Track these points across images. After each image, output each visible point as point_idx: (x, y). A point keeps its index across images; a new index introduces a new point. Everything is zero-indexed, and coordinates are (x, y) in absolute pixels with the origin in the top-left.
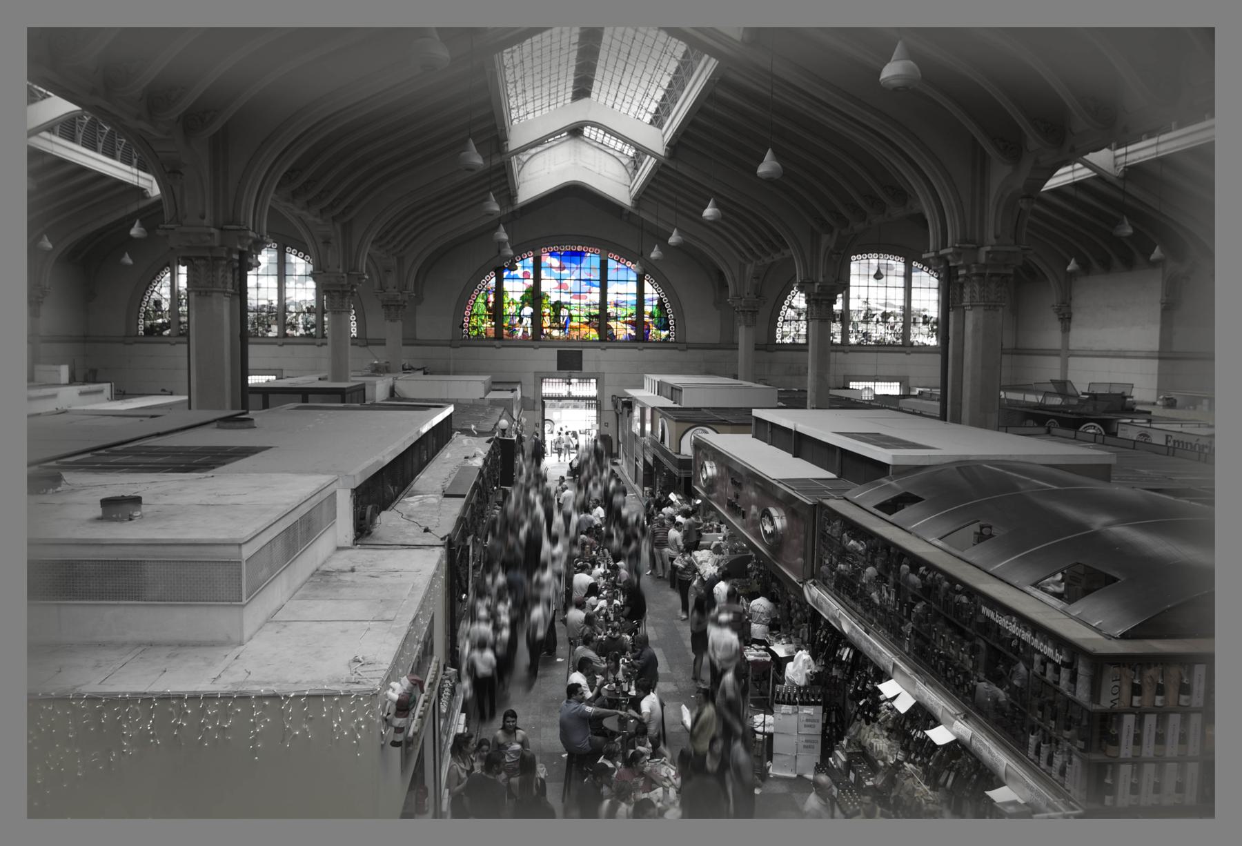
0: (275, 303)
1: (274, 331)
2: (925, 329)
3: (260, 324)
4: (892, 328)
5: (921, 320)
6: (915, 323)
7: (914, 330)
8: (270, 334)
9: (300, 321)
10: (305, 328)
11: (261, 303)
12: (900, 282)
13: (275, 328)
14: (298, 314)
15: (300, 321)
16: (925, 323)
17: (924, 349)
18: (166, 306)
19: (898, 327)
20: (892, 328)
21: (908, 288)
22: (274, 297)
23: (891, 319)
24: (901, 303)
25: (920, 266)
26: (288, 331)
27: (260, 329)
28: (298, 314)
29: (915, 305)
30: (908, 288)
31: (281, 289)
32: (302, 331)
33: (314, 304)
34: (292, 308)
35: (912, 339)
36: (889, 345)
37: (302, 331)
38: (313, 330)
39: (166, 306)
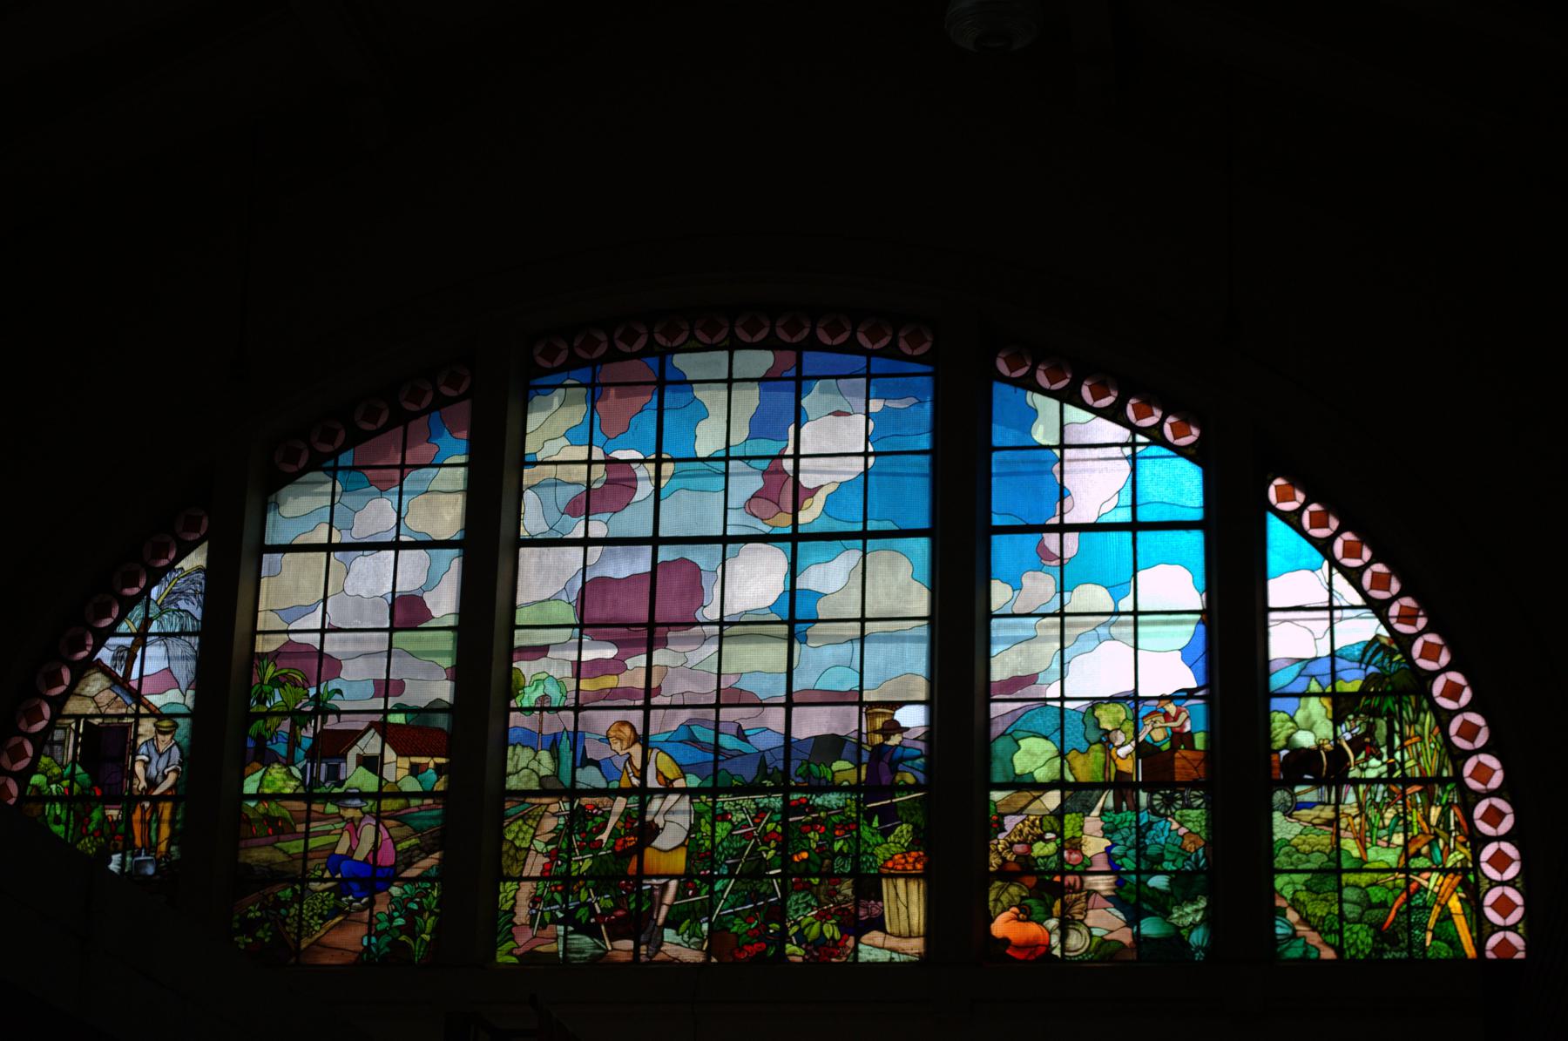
0: (913, 718)
1: (903, 922)
3: (795, 877)
8: (873, 949)
9: (1095, 845)
10: (1132, 902)
11: (812, 724)
13: (906, 905)
14: (1077, 794)
15: (1095, 845)
18: (157, 761)
22: (902, 668)
26: (1002, 926)
27: (804, 916)
28: (1077, 794)
31: (959, 626)
32: (1105, 922)
33: (1193, 719)
34: (1034, 757)
37: (1105, 922)
38: (1190, 914)
39: (157, 761)
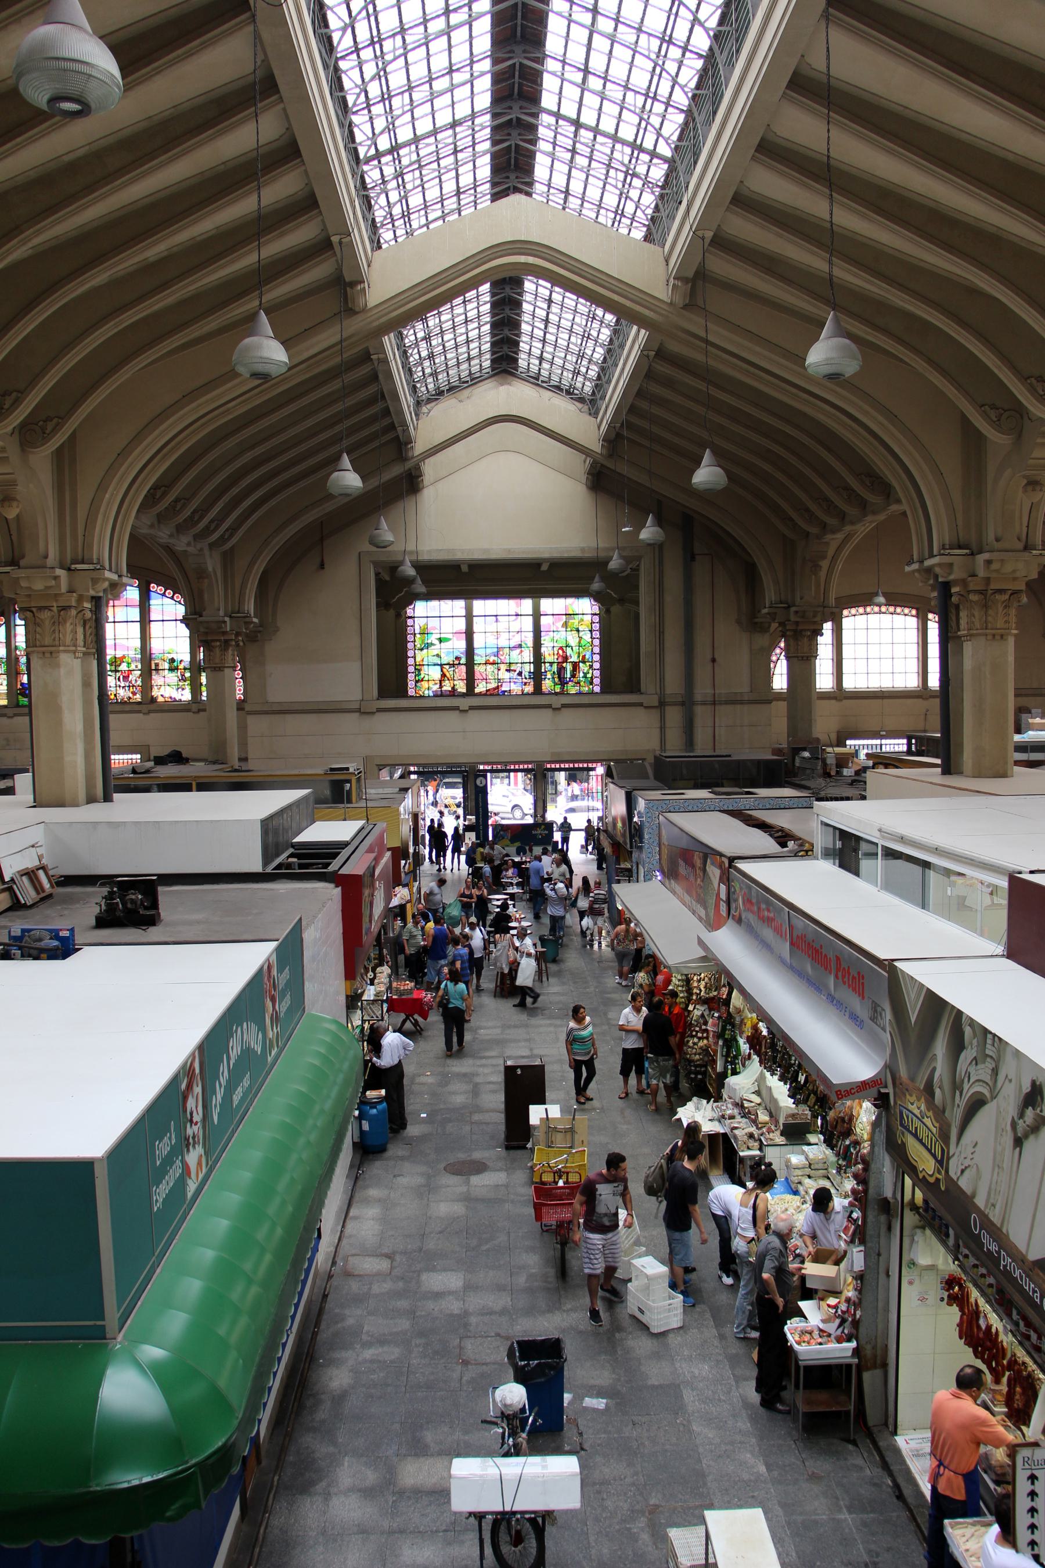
2: (173, 678)
4: (126, 678)
5: (167, 666)
6: (157, 670)
7: (157, 679)
12: (135, 614)
16: (171, 670)
17: (173, 707)
19: (135, 677)
20: (126, 678)
21: (145, 621)
23: (123, 667)
24: (137, 643)
25: (161, 589)
29: (156, 646)
30: (145, 621)
35: (155, 693)
36: (123, 703)
